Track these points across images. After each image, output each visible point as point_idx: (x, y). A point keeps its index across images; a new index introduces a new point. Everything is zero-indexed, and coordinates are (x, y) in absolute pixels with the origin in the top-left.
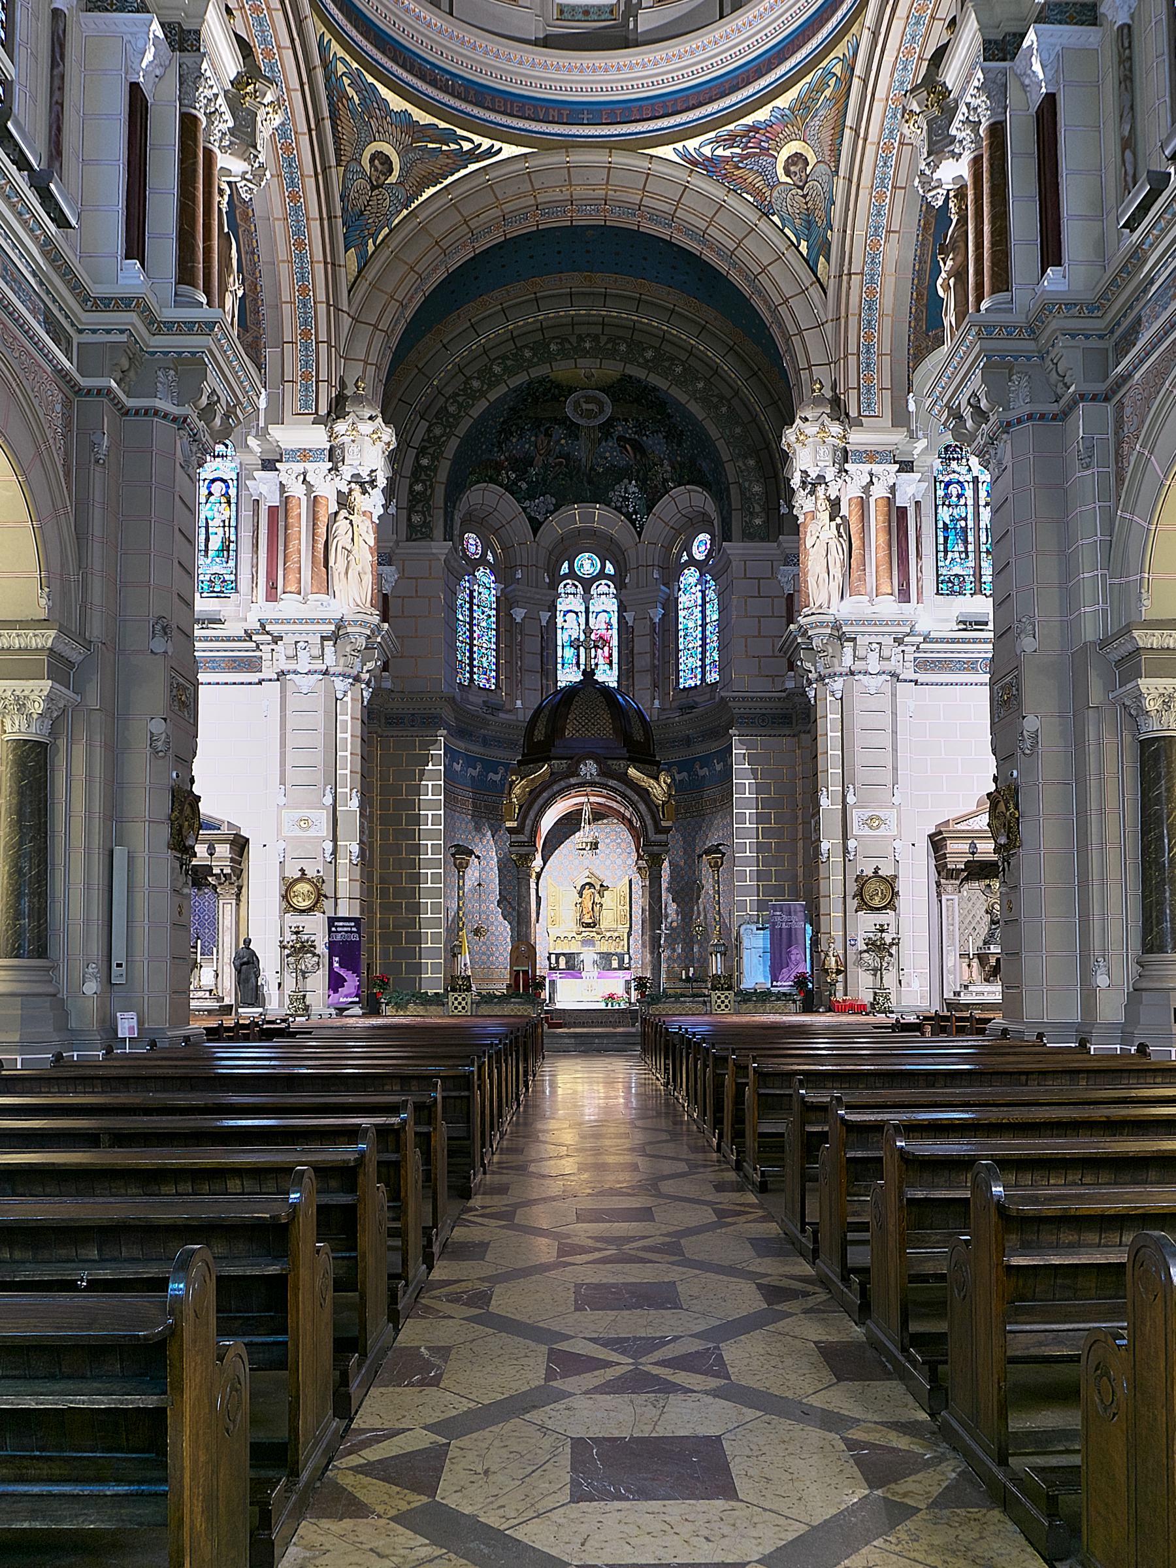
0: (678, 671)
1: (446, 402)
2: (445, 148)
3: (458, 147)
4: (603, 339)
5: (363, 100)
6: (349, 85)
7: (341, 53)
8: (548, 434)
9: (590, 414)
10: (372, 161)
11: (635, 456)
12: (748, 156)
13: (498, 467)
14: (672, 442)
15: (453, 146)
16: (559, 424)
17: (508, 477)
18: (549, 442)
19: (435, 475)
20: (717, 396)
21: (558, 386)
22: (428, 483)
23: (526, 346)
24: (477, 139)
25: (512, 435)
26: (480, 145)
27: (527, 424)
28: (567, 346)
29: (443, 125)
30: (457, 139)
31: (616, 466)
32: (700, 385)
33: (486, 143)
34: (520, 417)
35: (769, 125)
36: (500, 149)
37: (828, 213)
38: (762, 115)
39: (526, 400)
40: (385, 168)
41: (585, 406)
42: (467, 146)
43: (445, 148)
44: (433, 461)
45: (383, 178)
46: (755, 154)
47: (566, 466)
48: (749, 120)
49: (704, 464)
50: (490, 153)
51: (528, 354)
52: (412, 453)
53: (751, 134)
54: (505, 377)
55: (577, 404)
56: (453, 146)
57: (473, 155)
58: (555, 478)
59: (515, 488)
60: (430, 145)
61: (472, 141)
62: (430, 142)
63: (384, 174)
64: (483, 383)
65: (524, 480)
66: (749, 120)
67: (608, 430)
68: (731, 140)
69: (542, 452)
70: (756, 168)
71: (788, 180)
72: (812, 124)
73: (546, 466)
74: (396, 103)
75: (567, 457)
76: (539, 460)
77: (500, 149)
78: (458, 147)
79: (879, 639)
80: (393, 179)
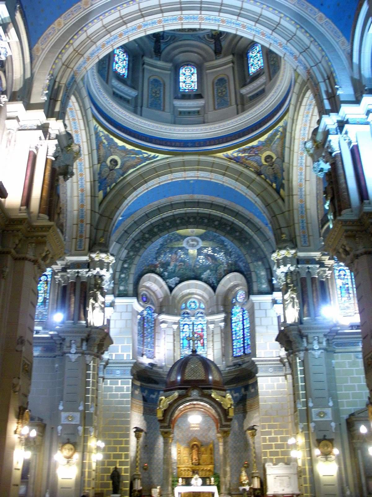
0: (233, 349)
2: (138, 156)
4: (198, 218)
5: (109, 143)
8: (176, 253)
10: (111, 161)
13: (156, 266)
15: (141, 156)
23: (167, 221)
24: (149, 153)
29: (137, 149)
30: (142, 153)
32: (238, 234)
33: (153, 154)
34: (164, 248)
35: (257, 147)
38: (255, 143)
39: (166, 241)
41: (191, 243)
42: (145, 155)
43: (138, 156)
48: (250, 145)
50: (154, 157)
51: (168, 224)
52: (121, 262)
55: (188, 242)
56: (141, 156)
57: (148, 158)
58: (179, 270)
59: (163, 274)
66: (250, 145)
68: (244, 151)
73: (176, 266)
74: (120, 143)
76: (172, 264)
79: (318, 335)
80: (118, 167)
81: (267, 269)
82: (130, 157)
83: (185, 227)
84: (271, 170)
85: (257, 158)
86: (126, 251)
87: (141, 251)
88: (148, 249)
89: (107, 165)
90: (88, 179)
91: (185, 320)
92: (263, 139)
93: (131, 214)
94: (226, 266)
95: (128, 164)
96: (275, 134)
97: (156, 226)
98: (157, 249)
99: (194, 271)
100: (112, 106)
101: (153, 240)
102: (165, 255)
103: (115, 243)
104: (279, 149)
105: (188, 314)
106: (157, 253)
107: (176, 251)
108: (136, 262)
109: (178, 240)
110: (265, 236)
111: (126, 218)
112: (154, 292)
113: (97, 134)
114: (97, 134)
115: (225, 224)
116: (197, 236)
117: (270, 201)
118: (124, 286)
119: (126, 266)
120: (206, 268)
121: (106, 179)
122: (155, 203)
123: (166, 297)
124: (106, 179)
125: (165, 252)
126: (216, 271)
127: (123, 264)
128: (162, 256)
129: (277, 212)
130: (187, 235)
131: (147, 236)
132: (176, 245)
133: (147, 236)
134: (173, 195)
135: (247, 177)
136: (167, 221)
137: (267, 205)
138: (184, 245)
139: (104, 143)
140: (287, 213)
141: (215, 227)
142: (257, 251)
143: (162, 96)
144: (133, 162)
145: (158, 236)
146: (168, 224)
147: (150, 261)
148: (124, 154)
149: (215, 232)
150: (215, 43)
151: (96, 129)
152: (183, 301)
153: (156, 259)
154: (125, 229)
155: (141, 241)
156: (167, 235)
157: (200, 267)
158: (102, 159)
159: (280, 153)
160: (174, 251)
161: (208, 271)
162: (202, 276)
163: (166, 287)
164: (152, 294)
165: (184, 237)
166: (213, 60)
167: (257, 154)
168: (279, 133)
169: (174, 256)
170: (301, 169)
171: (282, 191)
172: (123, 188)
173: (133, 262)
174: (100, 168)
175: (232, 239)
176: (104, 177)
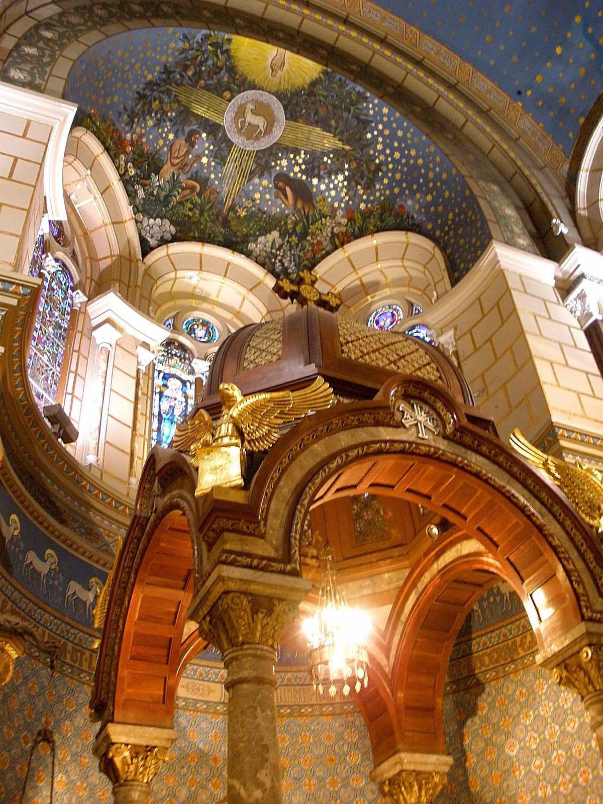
9: (251, 132)
11: (295, 204)
14: (358, 183)
16: (208, 134)
17: (126, 171)
18: (188, 153)
22: (47, 53)
25: (150, 113)
27: (172, 110)
31: (264, 213)
34: (169, 93)
39: (186, 68)
41: (250, 118)
47: (199, 195)
55: (241, 112)
58: (180, 203)
65: (144, 186)
67: (268, 162)
69: (176, 161)
73: (174, 182)
75: (204, 182)
76: (168, 171)
81: (517, 209)
83: (264, 39)
91: (172, 362)
94: (344, 221)
98: (149, 77)
99: (226, 223)
102: (158, 124)
105: (182, 347)
106: (141, 96)
107: (192, 133)
112: (86, 234)
116: (280, 96)
118: (31, 73)
120: (267, 224)
123: (125, 262)
125: (165, 113)
126: (303, 236)
138: (227, 121)
141: (352, 72)
152: (169, 310)
153: (131, 122)
156: (199, 35)
157: (251, 216)
160: (187, 129)
161: (275, 234)
162: (252, 246)
163: (131, 230)
164: (79, 232)
169: (181, 145)
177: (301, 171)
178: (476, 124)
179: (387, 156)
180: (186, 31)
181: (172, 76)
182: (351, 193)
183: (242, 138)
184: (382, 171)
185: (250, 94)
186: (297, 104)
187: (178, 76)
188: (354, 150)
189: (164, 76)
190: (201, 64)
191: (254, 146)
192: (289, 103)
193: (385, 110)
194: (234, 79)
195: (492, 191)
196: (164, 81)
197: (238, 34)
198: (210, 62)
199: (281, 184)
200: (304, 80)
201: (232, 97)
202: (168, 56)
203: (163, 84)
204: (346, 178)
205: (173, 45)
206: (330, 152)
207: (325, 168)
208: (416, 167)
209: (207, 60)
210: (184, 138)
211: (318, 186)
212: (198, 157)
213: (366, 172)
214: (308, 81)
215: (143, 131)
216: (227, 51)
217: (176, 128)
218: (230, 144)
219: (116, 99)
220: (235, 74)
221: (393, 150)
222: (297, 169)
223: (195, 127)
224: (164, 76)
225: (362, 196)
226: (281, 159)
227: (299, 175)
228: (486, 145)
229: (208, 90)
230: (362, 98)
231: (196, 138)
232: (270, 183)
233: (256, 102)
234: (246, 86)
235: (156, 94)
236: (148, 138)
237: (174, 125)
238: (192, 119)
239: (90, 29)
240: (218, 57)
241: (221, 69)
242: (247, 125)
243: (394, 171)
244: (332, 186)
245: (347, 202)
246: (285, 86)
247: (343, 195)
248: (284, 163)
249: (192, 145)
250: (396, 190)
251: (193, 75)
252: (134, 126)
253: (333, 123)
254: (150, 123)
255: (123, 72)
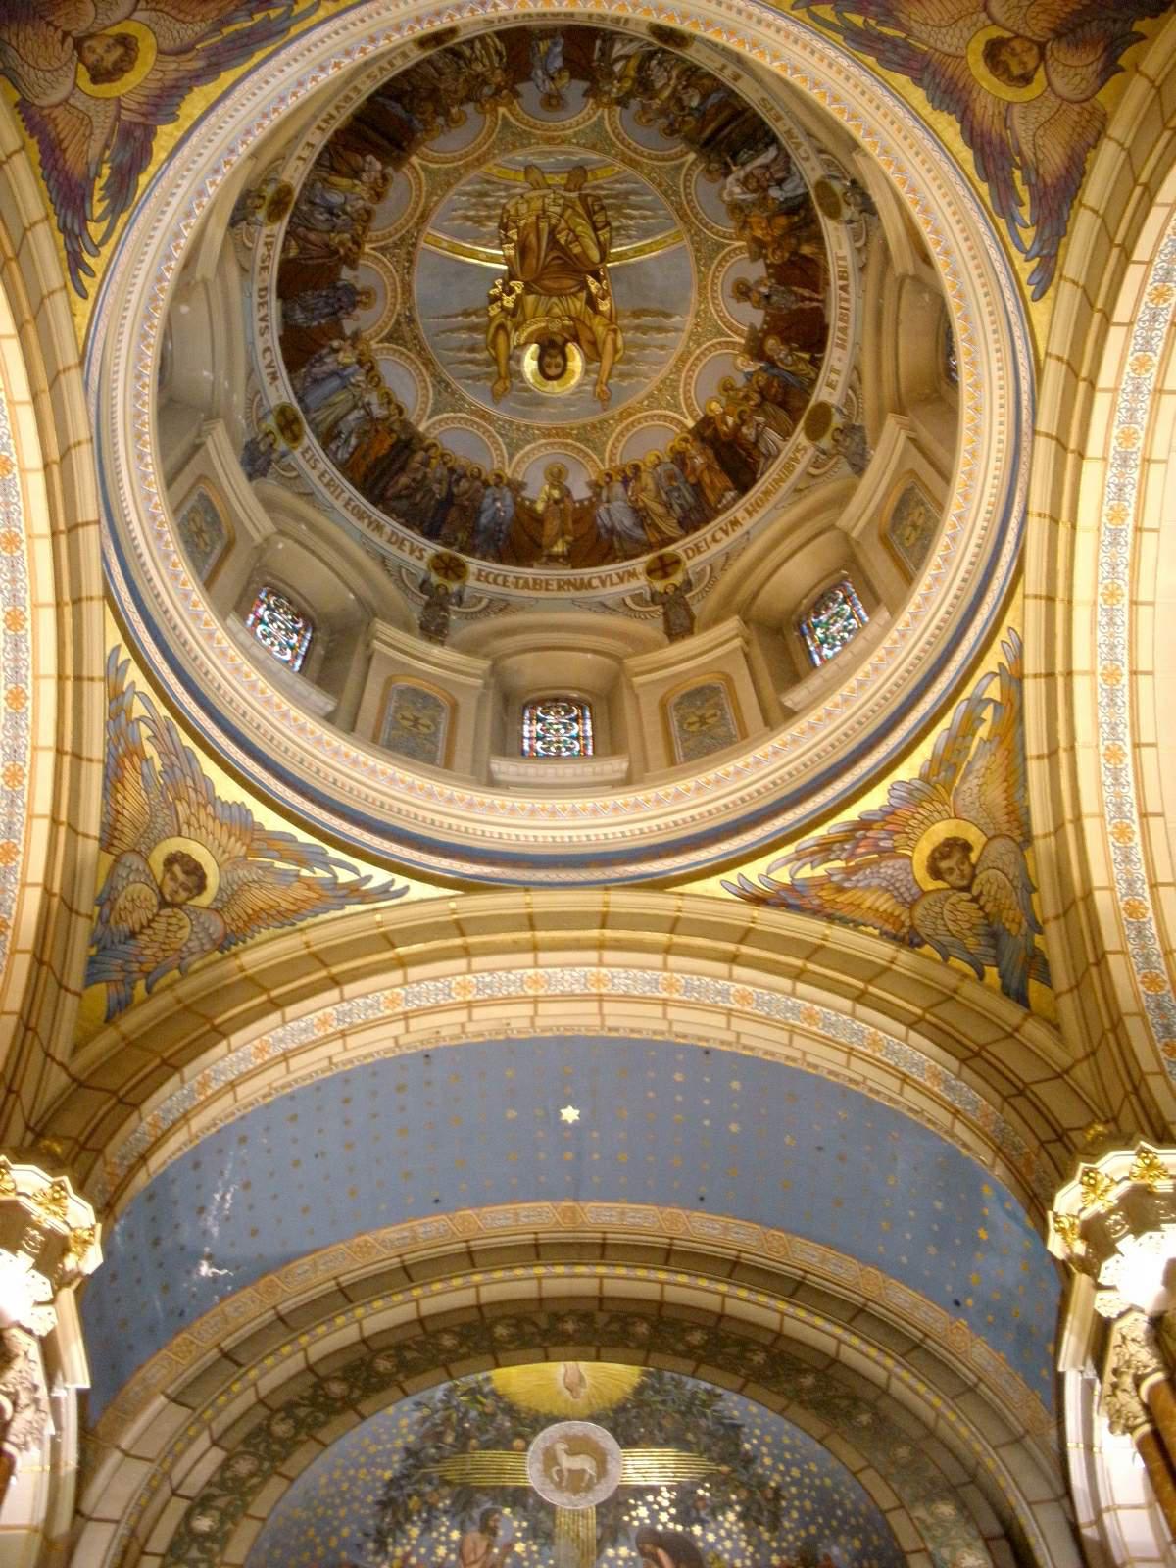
1: (269, 1419)
2: (305, 873)
3: (328, 875)
4: (601, 1319)
5: (169, 769)
6: (148, 739)
7: (143, 686)
8: (488, 1528)
9: (576, 1483)
10: (171, 861)
12: (859, 868)
14: (759, 1523)
15: (320, 873)
16: (512, 1506)
18: (489, 1547)
19: (223, 1550)
20: (846, 1397)
21: (511, 1410)
23: (446, 1330)
24: (365, 868)
25: (408, 1518)
26: (369, 878)
27: (442, 1498)
28: (529, 1329)
29: (303, 837)
30: (327, 863)
32: (808, 1381)
33: (380, 877)
35: (888, 814)
36: (406, 889)
37: (1028, 908)
38: (875, 800)
40: (191, 881)
41: (567, 1463)
42: (344, 876)
43: (305, 873)
44: (222, 1522)
45: (183, 894)
46: (870, 863)
48: (852, 814)
49: (835, 1551)
50: (385, 892)
51: (448, 1341)
52: (179, 1507)
53: (859, 834)
54: (400, 1377)
55: (550, 1458)
56: (320, 873)
57: (356, 892)
60: (279, 865)
61: (354, 870)
62: (281, 859)
63: (187, 889)
64: (351, 1387)
66: (852, 814)
68: (825, 849)
70: (875, 882)
71: (940, 884)
72: (965, 787)
74: (228, 789)
77: (406, 889)
78: (328, 875)
80: (205, 899)
81: (988, 1540)
82: (269, 869)
83: (539, 1352)
84: (964, 906)
85: (889, 868)
86: (217, 1456)
87: (299, 1457)
88: (334, 1449)
89: (150, 874)
90: (37, 873)
92: (909, 771)
93: (264, 1274)
95: (257, 898)
96: (971, 722)
97: (389, 1347)
98: (388, 1475)
100: (210, 636)
101: (364, 1407)
102: (428, 1526)
103: (161, 1400)
104: (996, 794)
106: (385, 1505)
107: (486, 1516)
108: (260, 1506)
109: (502, 1442)
110: (954, 1373)
111: (241, 1284)
113: (117, 698)
114: (117, 698)
115: (744, 1343)
116: (594, 1419)
117: (979, 1035)
119: (203, 1524)
121: (133, 935)
122: (390, 1233)
124: (133, 935)
125: (431, 1508)
127: (188, 1516)
128: (415, 1532)
129: (1027, 1072)
130: (544, 1409)
131: (337, 1388)
132: (491, 1465)
133: (337, 1388)
134: (479, 1204)
135: (847, 962)
136: (446, 1330)
137: (970, 1056)
138: (533, 1475)
139: (146, 760)
140: (1082, 1073)
141: (689, 1352)
142: (918, 1452)
143: (442, 744)
144: (282, 897)
145: (394, 1392)
146: (448, 1341)
147: (344, 1543)
148: (239, 849)
149: (693, 1375)
150: (665, 614)
151: (114, 672)
154: (228, 1344)
155: (302, 1412)
156: (439, 1393)
158: (129, 836)
159: (1001, 817)
160: (476, 1514)
165: (526, 1423)
166: (659, 646)
167: (890, 853)
168: (988, 713)
170: (1123, 833)
171: (1034, 987)
172: (222, 993)
173: (246, 1506)
174: (112, 872)
175: (782, 1402)
176: (125, 927)
177: (673, 1518)
178: (900, 1379)
179: (783, 1474)
180: (417, 1398)
181: (422, 1456)
182: (754, 1540)
183: (566, 1494)
184: (784, 1498)
185: (553, 1430)
186: (628, 1422)
187: (433, 1451)
188: (734, 1471)
189: (411, 1461)
190: (461, 1420)
191: (588, 1503)
192: (617, 1424)
193: (754, 1409)
194: (519, 1419)
195: (941, 1522)
196: (415, 1467)
197: (498, 1365)
198: (473, 1414)
199: (648, 1547)
200: (623, 1390)
201: (528, 1443)
202: (403, 1436)
203: (412, 1471)
204: (741, 1517)
205: (404, 1422)
206: (704, 1480)
207: (705, 1506)
208: (821, 1489)
209: (466, 1414)
210: (474, 1528)
211: (703, 1537)
212: (508, 1548)
213: (764, 1503)
214: (629, 1389)
215: (408, 1549)
216: (493, 1392)
217: (458, 1519)
218: (551, 1510)
219: (345, 1532)
220: (519, 1412)
221: (788, 1464)
222: (664, 1517)
223: (488, 1506)
224: (411, 1461)
225: (769, 1542)
226: (635, 1507)
227: (671, 1525)
228: (929, 1415)
229: (488, 1448)
230: (713, 1396)
231: (496, 1520)
232: (631, 1549)
233: (568, 1439)
234: (543, 1421)
235: (408, 1489)
236: (418, 1555)
237: (453, 1516)
238: (478, 1496)
239: (266, 1478)
240: (481, 1403)
241: (493, 1415)
242: (566, 1474)
243: (800, 1497)
244: (723, 1532)
245: (752, 1556)
246: (599, 1404)
247: (743, 1544)
248: (643, 1512)
249: (493, 1532)
250: (813, 1529)
251: (456, 1438)
252: (390, 1549)
253: (690, 1436)
254: (415, 1532)
255: (341, 1494)
